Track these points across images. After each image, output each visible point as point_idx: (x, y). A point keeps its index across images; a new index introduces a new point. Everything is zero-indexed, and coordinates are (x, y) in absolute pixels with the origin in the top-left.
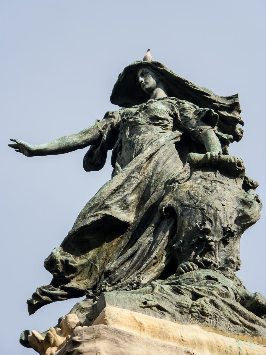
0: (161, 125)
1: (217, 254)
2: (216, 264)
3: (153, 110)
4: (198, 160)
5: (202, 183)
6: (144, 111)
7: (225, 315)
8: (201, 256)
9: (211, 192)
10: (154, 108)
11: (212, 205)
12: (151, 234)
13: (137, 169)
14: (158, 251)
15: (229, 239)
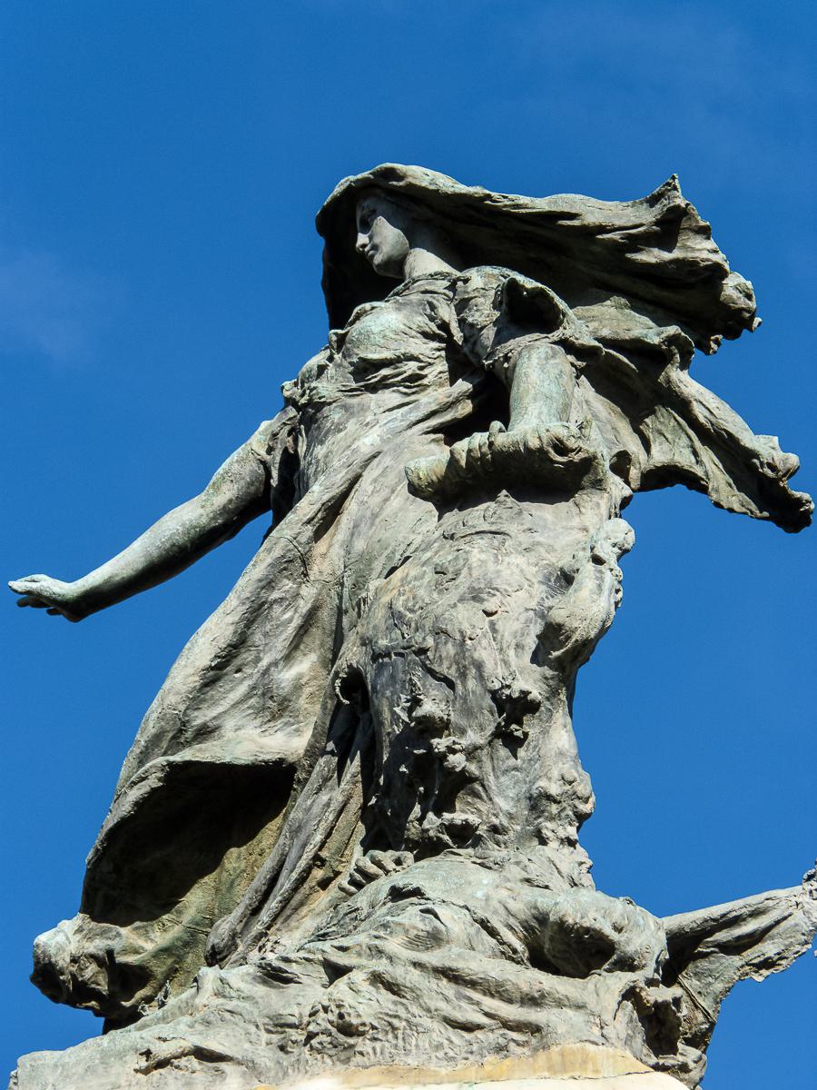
0: (393, 385)
1: (493, 788)
2: (496, 821)
4: (434, 478)
7: (429, 1010)
8: (438, 814)
10: (360, 334)
11: (449, 627)
13: (285, 569)
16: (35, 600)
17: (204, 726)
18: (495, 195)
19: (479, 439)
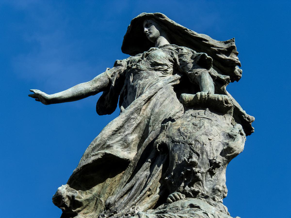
1: (205, 184)
2: (204, 193)
3: (154, 57)
4: (189, 100)
5: (192, 121)
6: (146, 59)
8: (189, 187)
9: (199, 128)
10: (155, 55)
11: (199, 140)
12: (147, 168)
13: (136, 111)
14: (151, 184)
15: (215, 170)
16: (38, 97)
17: (109, 145)
18: (188, 29)
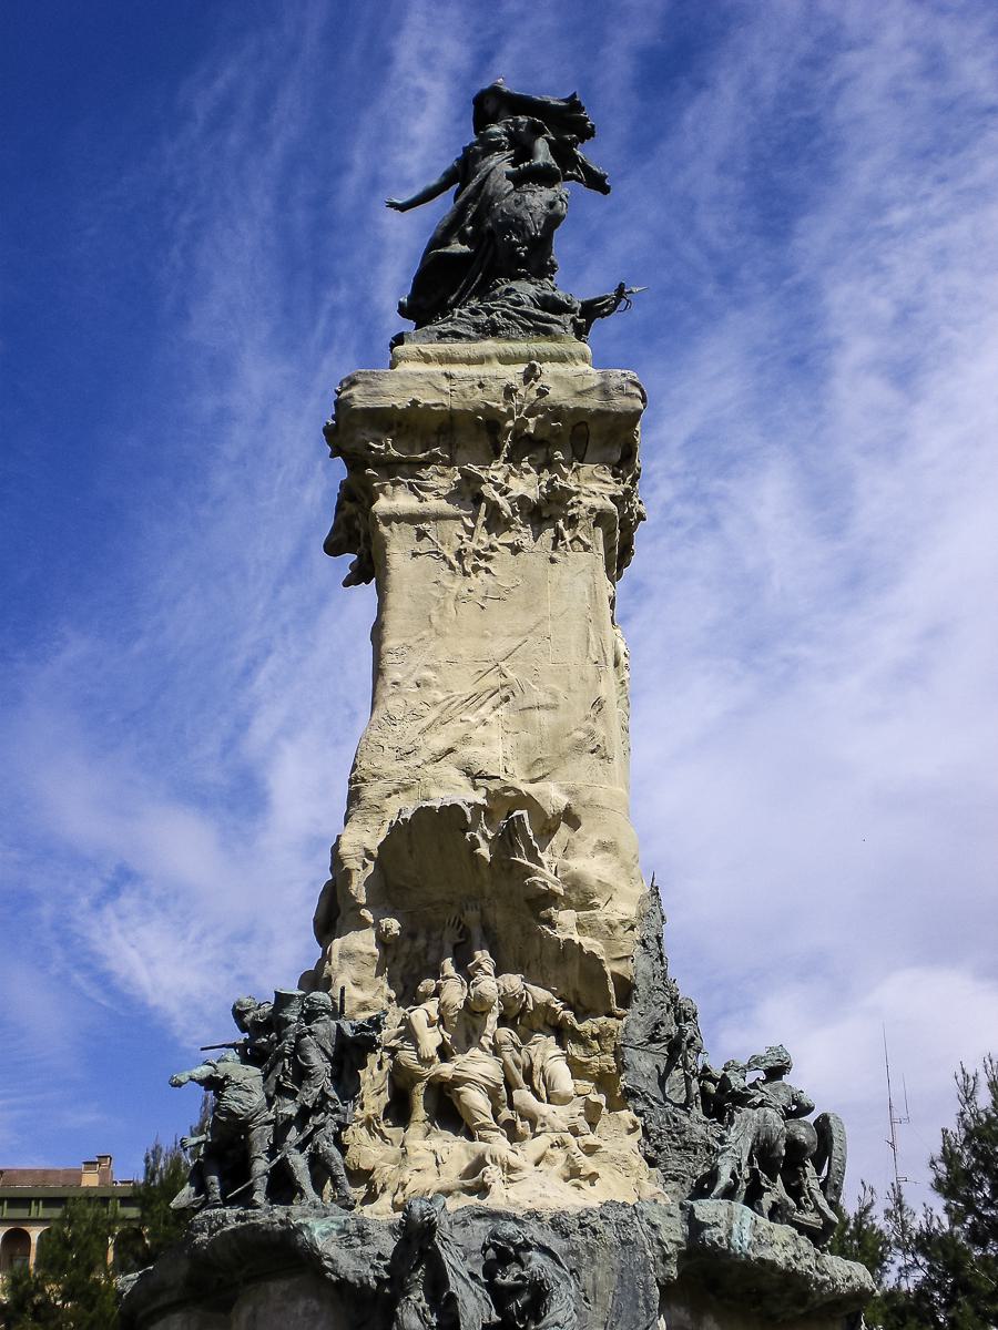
19: (526, 164)
